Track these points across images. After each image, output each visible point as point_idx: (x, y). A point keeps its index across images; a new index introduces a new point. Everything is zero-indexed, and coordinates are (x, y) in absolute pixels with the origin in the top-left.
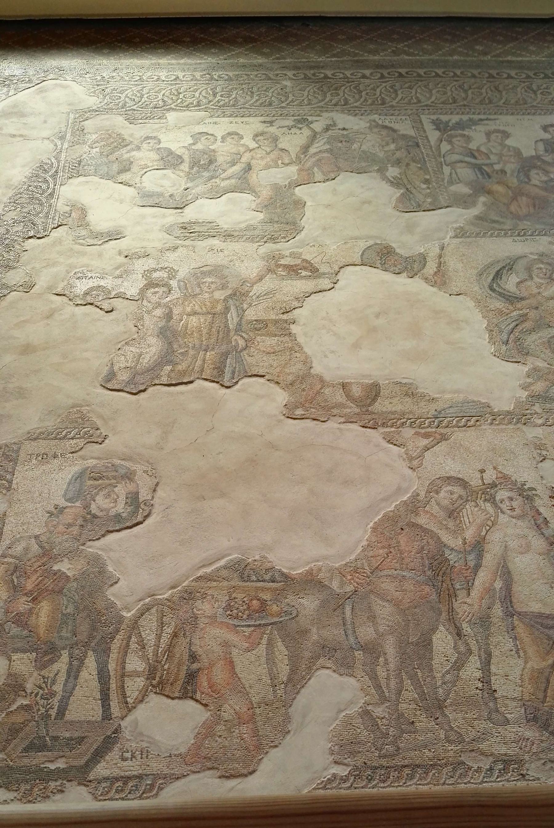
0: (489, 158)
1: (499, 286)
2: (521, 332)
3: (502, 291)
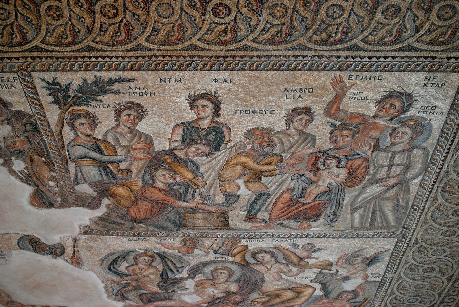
0: (116, 153)
1: (114, 268)
2: (125, 291)
3: (116, 271)
